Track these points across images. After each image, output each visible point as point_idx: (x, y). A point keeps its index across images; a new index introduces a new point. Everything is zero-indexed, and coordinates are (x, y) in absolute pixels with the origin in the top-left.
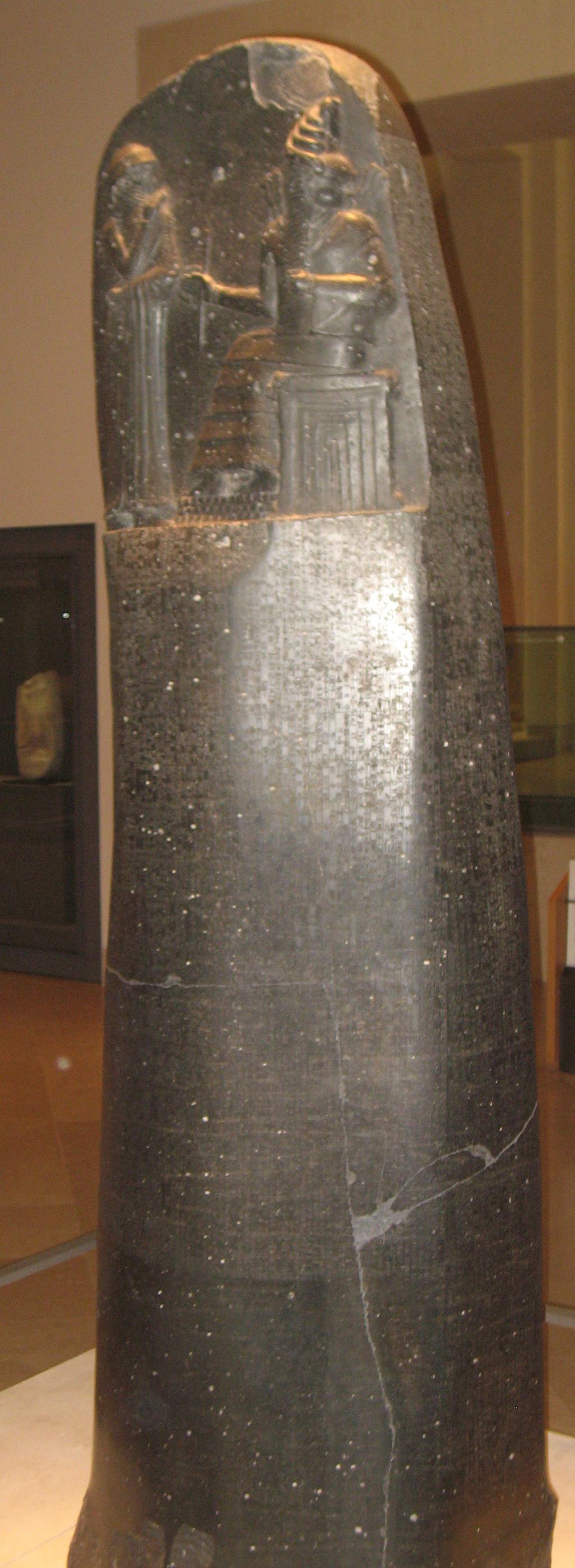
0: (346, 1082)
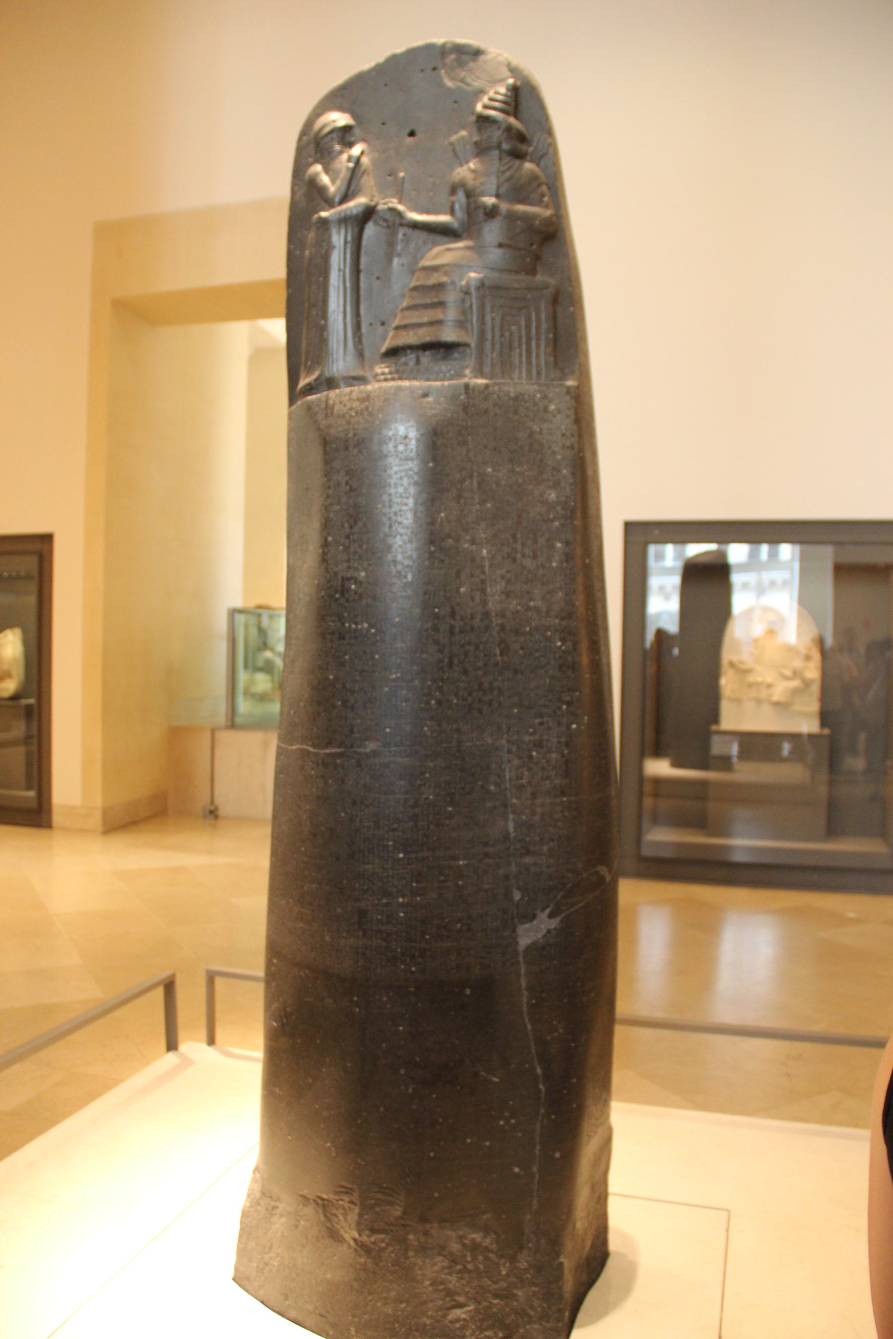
0: (514, 820)
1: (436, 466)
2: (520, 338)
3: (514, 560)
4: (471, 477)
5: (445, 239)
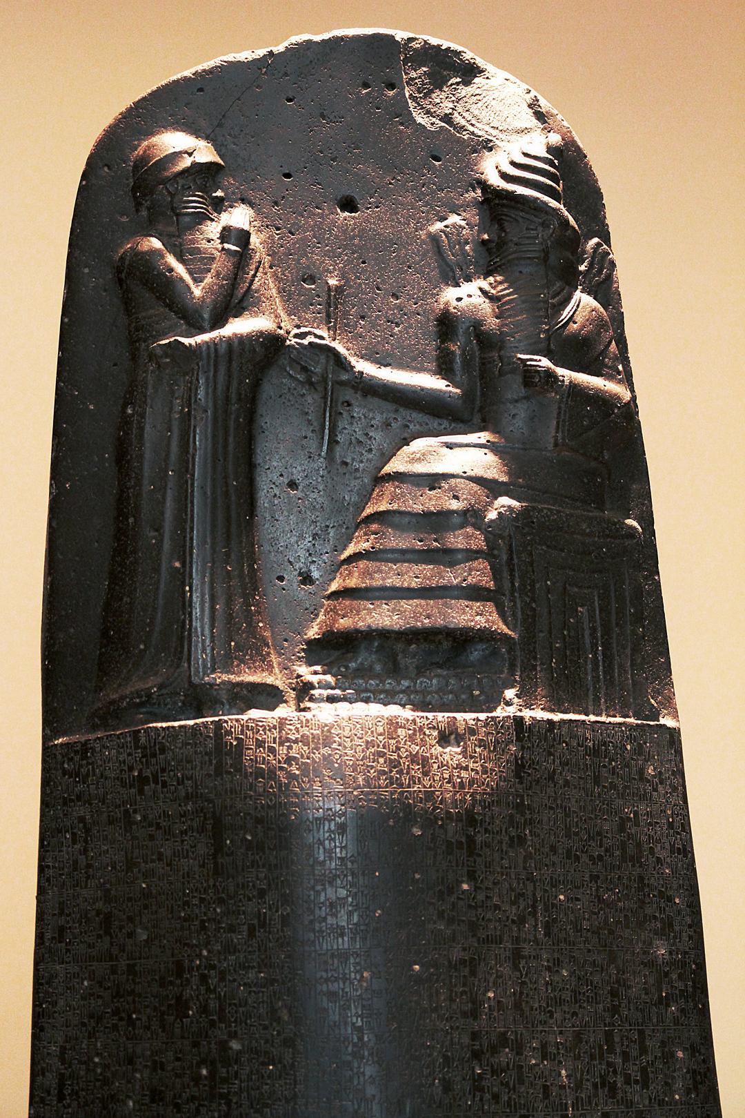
1: (477, 888)
2: (593, 630)
3: (613, 1089)
4: (534, 914)
5: (435, 424)
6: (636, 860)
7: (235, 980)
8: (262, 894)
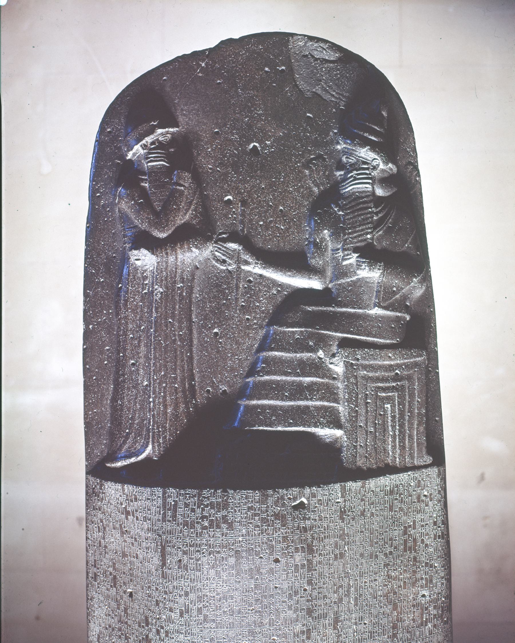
2: (393, 417)
4: (348, 595)
6: (413, 549)
7: (173, 638)
8: (187, 594)
